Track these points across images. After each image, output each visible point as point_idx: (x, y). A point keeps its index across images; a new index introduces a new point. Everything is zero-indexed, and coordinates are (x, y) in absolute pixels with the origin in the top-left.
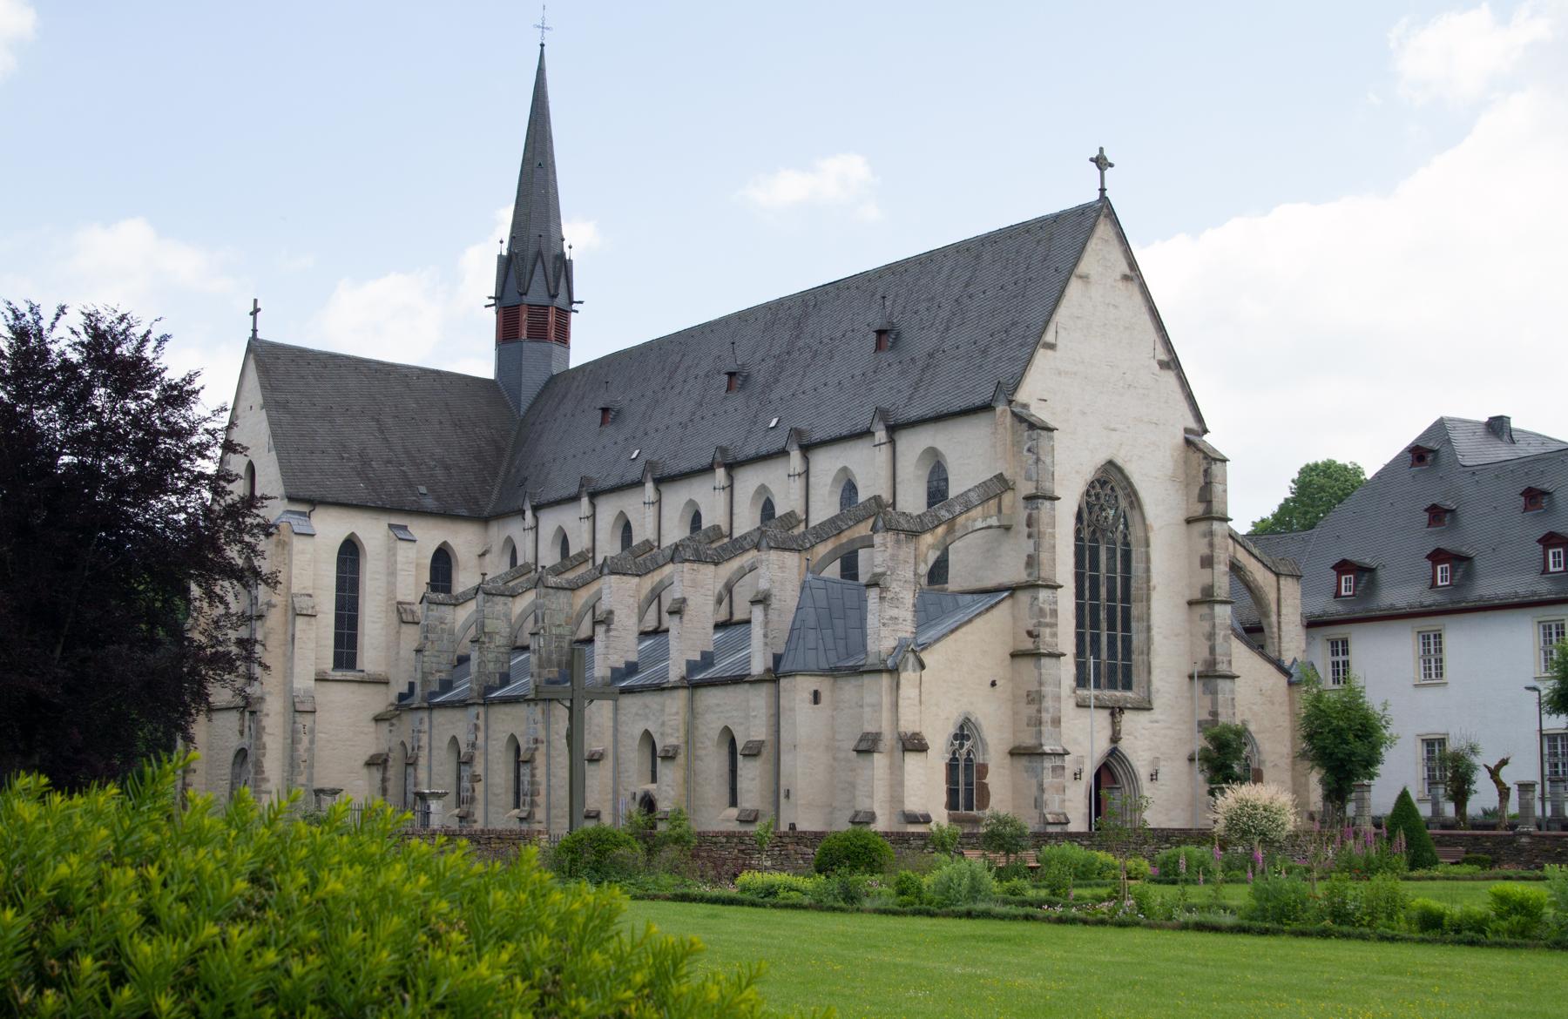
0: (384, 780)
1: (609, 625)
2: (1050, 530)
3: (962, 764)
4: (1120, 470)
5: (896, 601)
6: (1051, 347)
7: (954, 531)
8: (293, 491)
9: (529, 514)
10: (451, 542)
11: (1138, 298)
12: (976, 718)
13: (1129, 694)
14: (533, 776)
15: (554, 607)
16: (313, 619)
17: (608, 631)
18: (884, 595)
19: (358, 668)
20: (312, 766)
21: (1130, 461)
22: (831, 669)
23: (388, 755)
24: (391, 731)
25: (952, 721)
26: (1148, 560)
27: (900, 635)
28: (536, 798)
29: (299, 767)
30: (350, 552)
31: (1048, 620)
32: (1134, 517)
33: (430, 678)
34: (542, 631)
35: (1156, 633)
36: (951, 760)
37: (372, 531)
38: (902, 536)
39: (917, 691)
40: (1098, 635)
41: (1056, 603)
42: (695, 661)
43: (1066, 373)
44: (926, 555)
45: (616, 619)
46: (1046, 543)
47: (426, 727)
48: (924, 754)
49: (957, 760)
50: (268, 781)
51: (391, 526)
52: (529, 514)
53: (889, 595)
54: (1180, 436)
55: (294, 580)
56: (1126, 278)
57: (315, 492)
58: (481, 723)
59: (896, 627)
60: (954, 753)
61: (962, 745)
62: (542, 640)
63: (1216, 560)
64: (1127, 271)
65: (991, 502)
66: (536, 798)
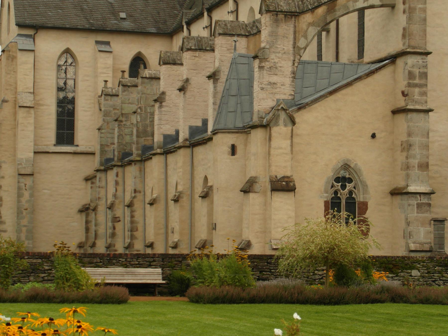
0: (87, 222)
1: (161, 103)
5: (273, 69)
7: (335, 11)
8: (21, 21)
9: (185, 27)
10: (144, 52)
12: (356, 164)
14: (132, 217)
15: (148, 92)
16: (32, 111)
17: (161, 107)
18: (263, 64)
19: (75, 144)
20: (33, 212)
22: (244, 127)
23: (89, 205)
24: (91, 187)
27: (278, 97)
28: (135, 233)
29: (22, 213)
31: (417, 81)
33: (106, 149)
34: (139, 110)
36: (332, 198)
38: (281, 16)
39: (289, 142)
41: (426, 67)
42: (197, 127)
44: (306, 31)
45: (167, 98)
47: (103, 184)
48: (292, 194)
49: (339, 198)
52: (185, 27)
53: (267, 65)
55: (19, 83)
57: (40, 20)
58: (120, 179)
59: (275, 91)
60: (336, 193)
61: (344, 187)
62: (138, 117)
66: (135, 233)
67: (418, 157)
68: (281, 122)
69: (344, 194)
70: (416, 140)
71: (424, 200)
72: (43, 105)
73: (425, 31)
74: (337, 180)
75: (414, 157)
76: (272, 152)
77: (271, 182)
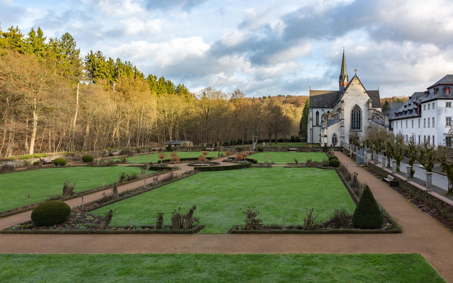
6: (347, 93)
26: (362, 115)
30: (318, 113)
32: (360, 110)
35: (363, 123)
37: (320, 110)
56: (359, 83)
69: (335, 137)
70: (342, 130)
71: (343, 138)
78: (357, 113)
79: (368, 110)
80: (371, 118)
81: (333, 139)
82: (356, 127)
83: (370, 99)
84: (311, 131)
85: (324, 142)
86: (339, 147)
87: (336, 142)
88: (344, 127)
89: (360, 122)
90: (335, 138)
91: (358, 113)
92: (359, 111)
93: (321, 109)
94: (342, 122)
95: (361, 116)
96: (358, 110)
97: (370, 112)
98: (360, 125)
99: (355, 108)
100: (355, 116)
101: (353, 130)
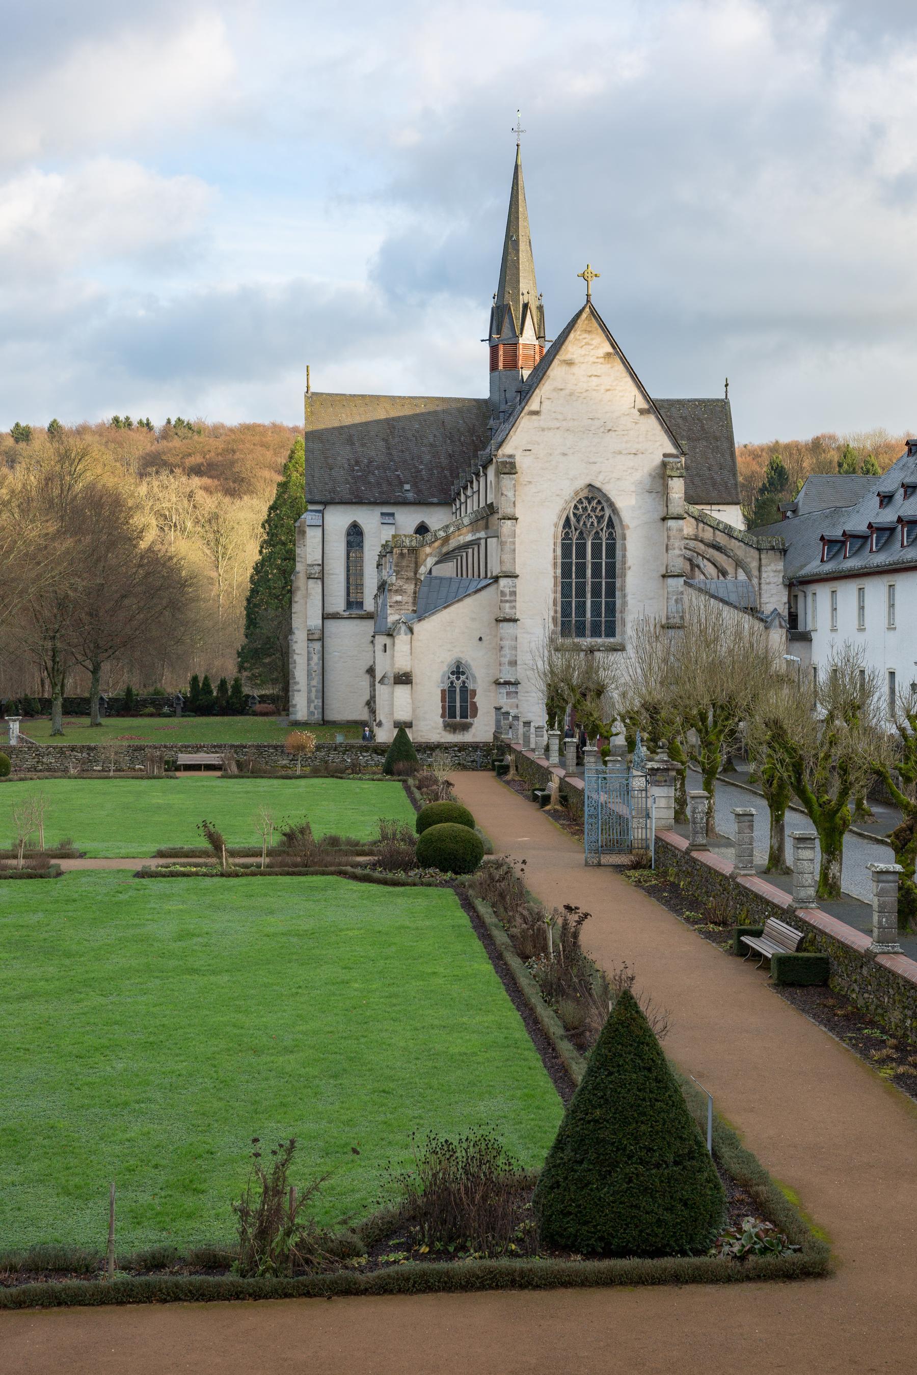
2: (511, 540)
3: (458, 690)
4: (599, 490)
6: (536, 413)
11: (621, 367)
13: (612, 640)
21: (608, 482)
25: (446, 664)
30: (355, 534)
31: (508, 598)
32: (614, 518)
35: (629, 598)
36: (449, 687)
39: (409, 646)
40: (585, 602)
41: (515, 587)
43: (550, 429)
46: (508, 547)
48: (409, 686)
49: (455, 687)
50: (298, 683)
51: (382, 514)
54: (658, 459)
56: (608, 355)
60: (452, 683)
61: (458, 678)
63: (670, 547)
64: (611, 350)
65: (480, 522)
67: (508, 656)
68: (402, 631)
69: (458, 684)
70: (506, 643)
71: (512, 689)
72: (333, 574)
73: (514, 559)
74: (453, 673)
75: (505, 656)
76: (396, 654)
77: (395, 678)
78: (597, 535)
79: (664, 519)
80: (677, 571)
81: (448, 695)
82: (588, 625)
83: (671, 450)
84: (317, 646)
85: (392, 713)
86: (486, 744)
87: (464, 715)
88: (515, 621)
89: (611, 591)
90: (464, 689)
91: (604, 535)
92: (611, 524)
93: (378, 510)
94: (503, 594)
95: (619, 553)
96: (600, 519)
97: (673, 533)
98: (611, 609)
99: (585, 509)
100: (581, 553)
101: (568, 641)
